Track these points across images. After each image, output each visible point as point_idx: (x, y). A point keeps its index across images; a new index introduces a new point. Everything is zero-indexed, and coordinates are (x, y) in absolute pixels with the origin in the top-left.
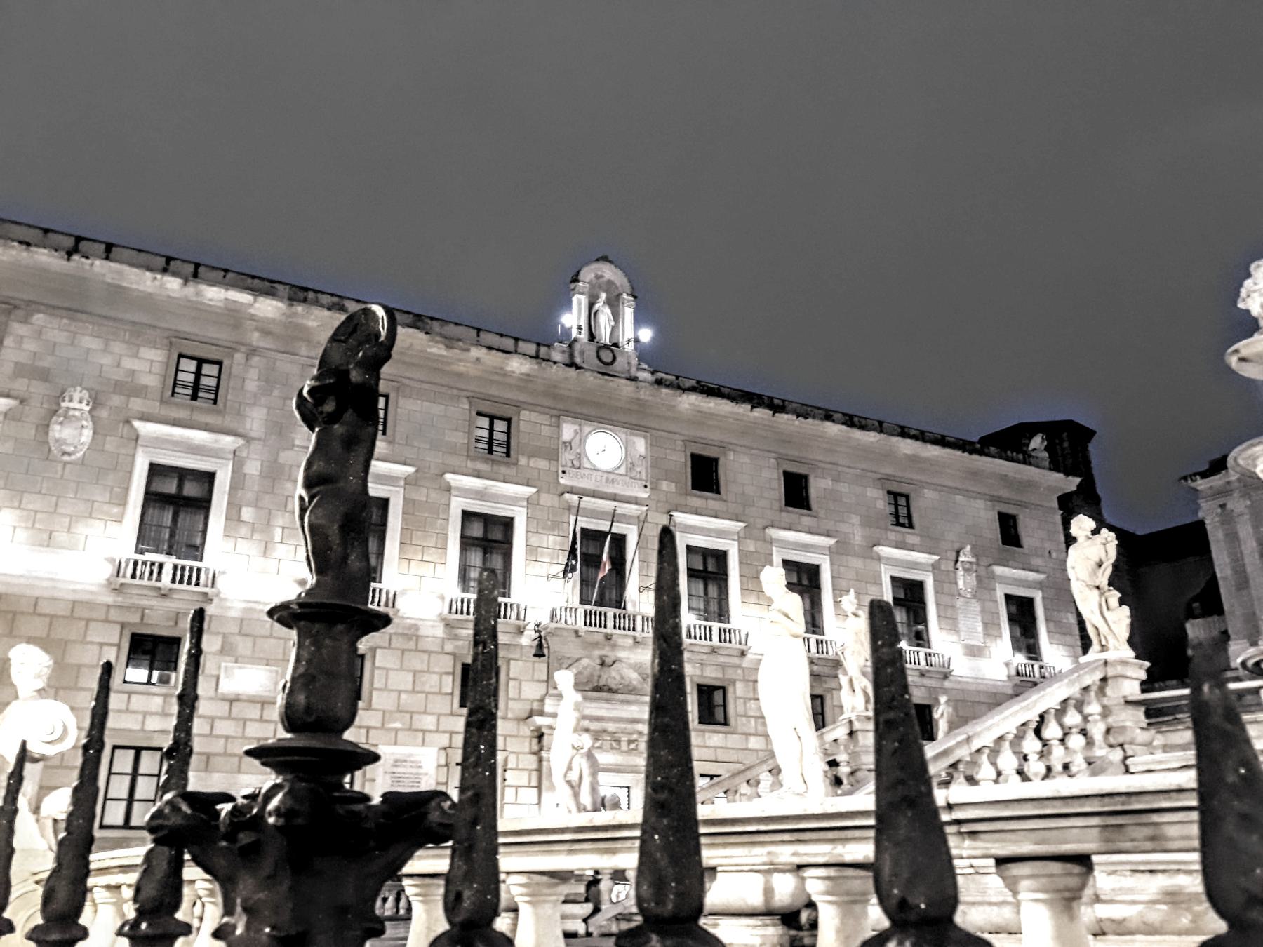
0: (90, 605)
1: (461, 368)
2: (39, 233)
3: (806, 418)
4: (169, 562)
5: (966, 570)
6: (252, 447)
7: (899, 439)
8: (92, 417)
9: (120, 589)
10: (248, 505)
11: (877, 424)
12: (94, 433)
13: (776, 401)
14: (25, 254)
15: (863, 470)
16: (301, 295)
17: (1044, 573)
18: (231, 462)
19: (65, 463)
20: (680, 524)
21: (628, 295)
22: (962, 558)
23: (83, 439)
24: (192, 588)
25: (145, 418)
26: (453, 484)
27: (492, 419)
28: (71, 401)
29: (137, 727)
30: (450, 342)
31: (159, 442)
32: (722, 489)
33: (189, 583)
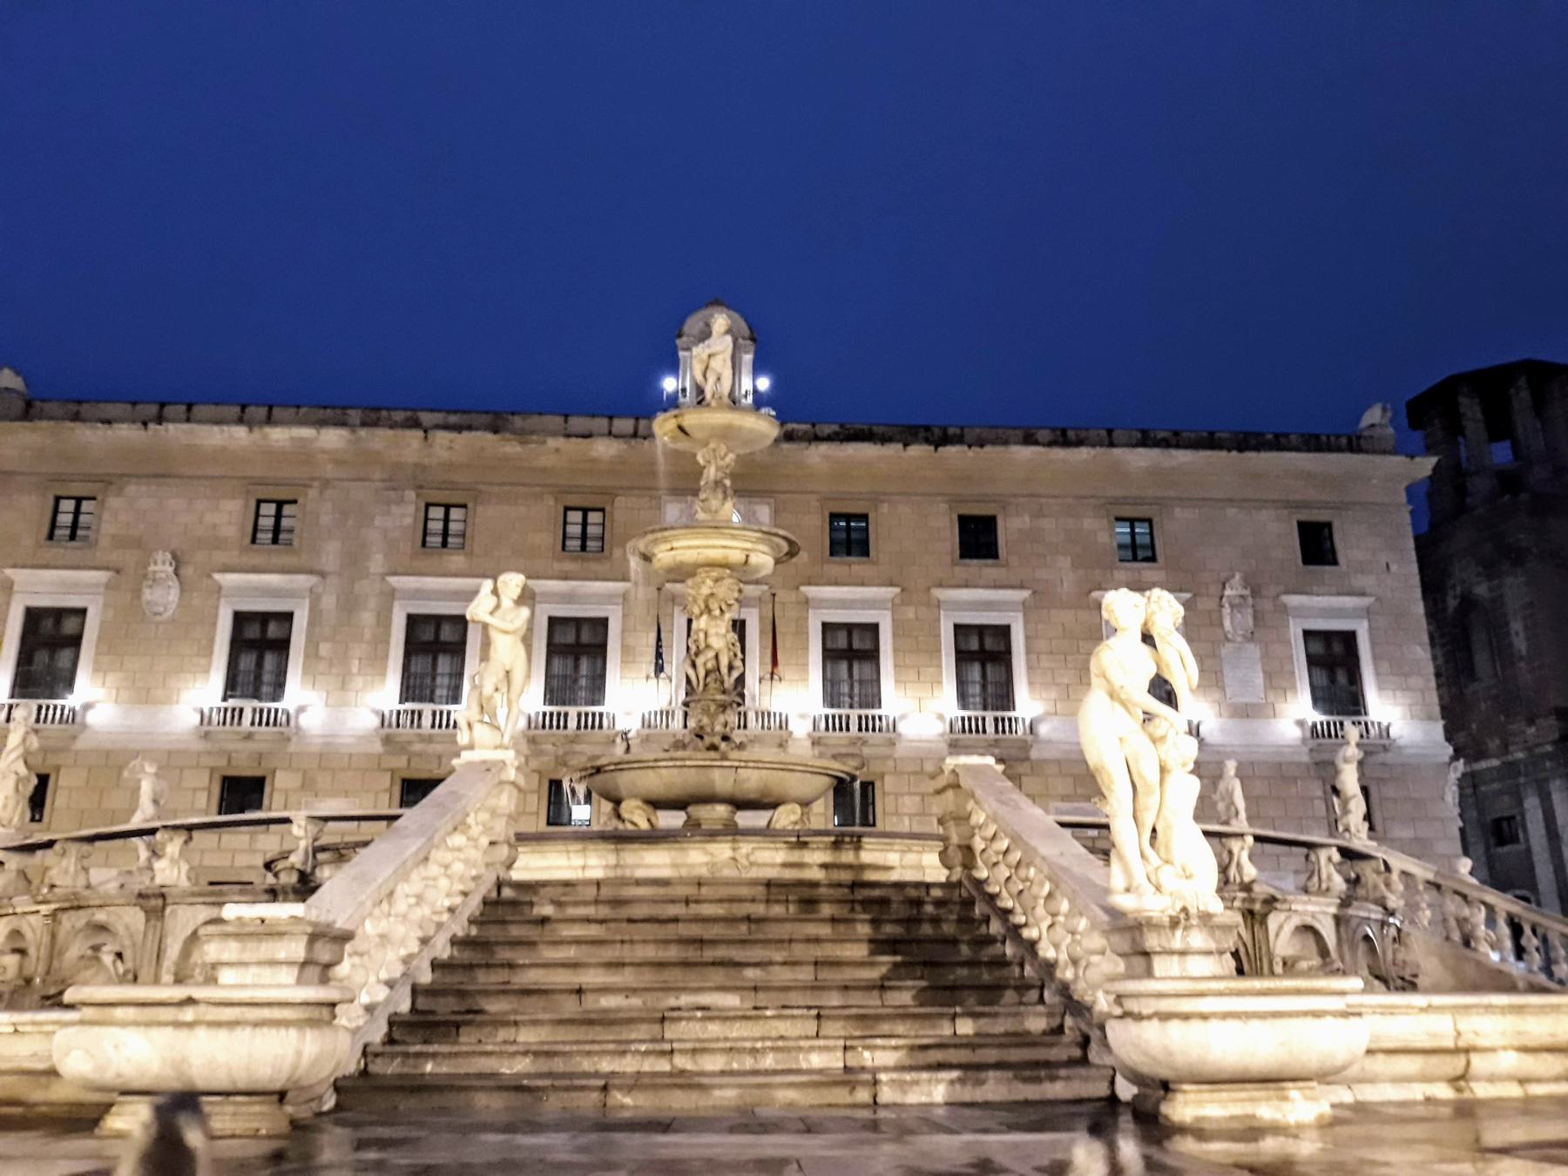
0: (179, 752)
1: (546, 460)
2: (129, 407)
3: (982, 446)
4: (249, 705)
5: (1232, 606)
6: (328, 581)
7: (1126, 450)
8: (177, 575)
9: (206, 736)
10: (326, 640)
11: (1103, 433)
12: (182, 591)
13: (951, 431)
14: (109, 432)
15: (1077, 497)
16: (373, 416)
17: (1371, 595)
18: (307, 602)
19: (158, 624)
20: (813, 599)
21: (744, 338)
22: (1228, 592)
23: (171, 598)
24: (271, 729)
25: (227, 569)
26: (537, 590)
27: (585, 511)
28: (155, 563)
29: (227, 863)
30: (522, 435)
31: (240, 591)
32: (872, 552)
33: (268, 724)
